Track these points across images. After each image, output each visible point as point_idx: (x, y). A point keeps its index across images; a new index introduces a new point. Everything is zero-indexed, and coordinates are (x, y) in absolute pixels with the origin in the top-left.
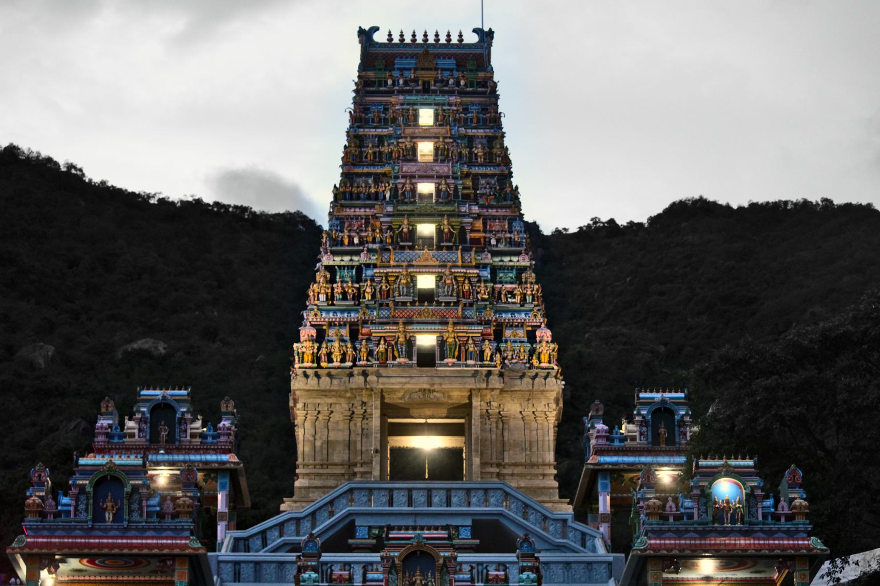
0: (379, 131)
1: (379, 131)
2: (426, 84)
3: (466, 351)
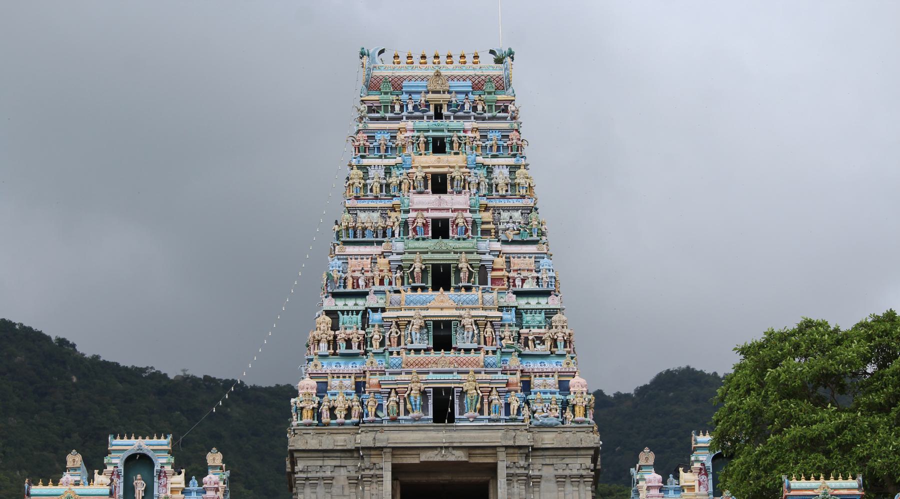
2: (438, 108)
3: (490, 403)
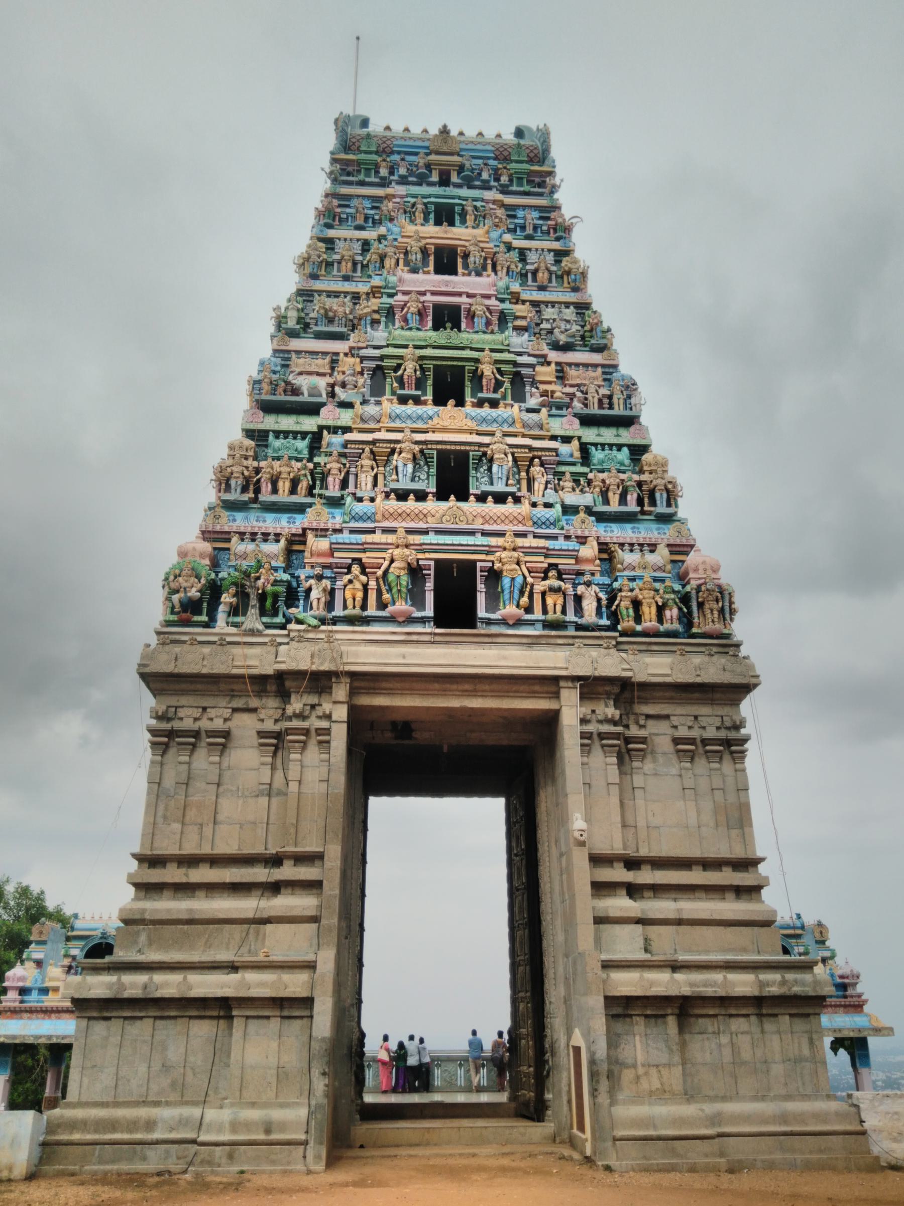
0: (364, 235)
1: (364, 235)
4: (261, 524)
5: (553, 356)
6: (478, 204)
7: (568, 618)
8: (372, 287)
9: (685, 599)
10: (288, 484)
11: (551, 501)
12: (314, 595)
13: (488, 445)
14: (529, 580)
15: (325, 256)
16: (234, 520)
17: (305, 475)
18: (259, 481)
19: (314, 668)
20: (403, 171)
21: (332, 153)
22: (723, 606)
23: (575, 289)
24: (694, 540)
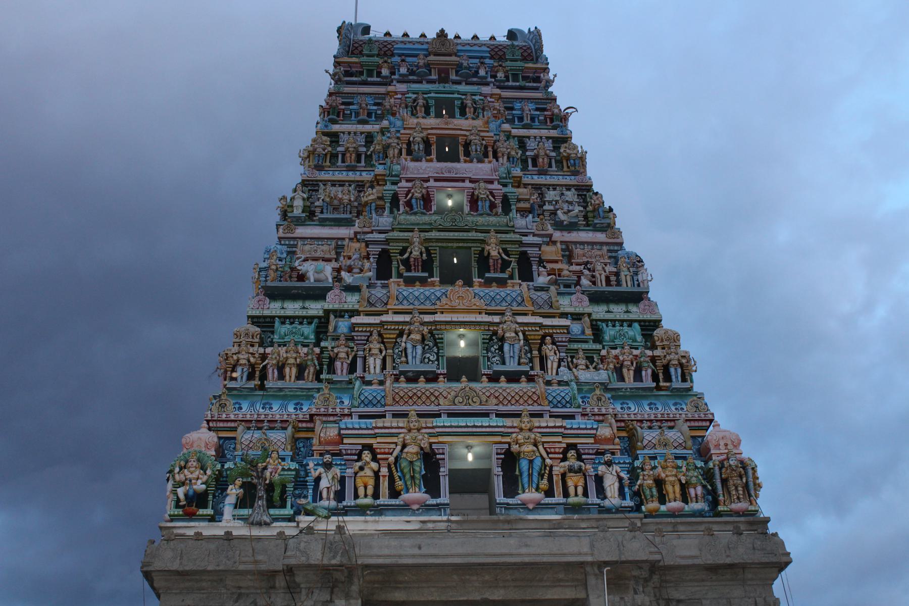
0: (368, 128)
1: (368, 128)
4: (267, 412)
5: (557, 235)
6: (477, 98)
7: (590, 501)
8: (376, 175)
9: (708, 475)
10: (294, 370)
11: (565, 378)
12: (324, 484)
13: (498, 324)
14: (548, 461)
15: (330, 149)
16: (240, 408)
17: (312, 360)
18: (265, 367)
19: (325, 562)
20: (403, 70)
21: (334, 57)
22: (747, 482)
23: (575, 173)
24: (713, 414)
